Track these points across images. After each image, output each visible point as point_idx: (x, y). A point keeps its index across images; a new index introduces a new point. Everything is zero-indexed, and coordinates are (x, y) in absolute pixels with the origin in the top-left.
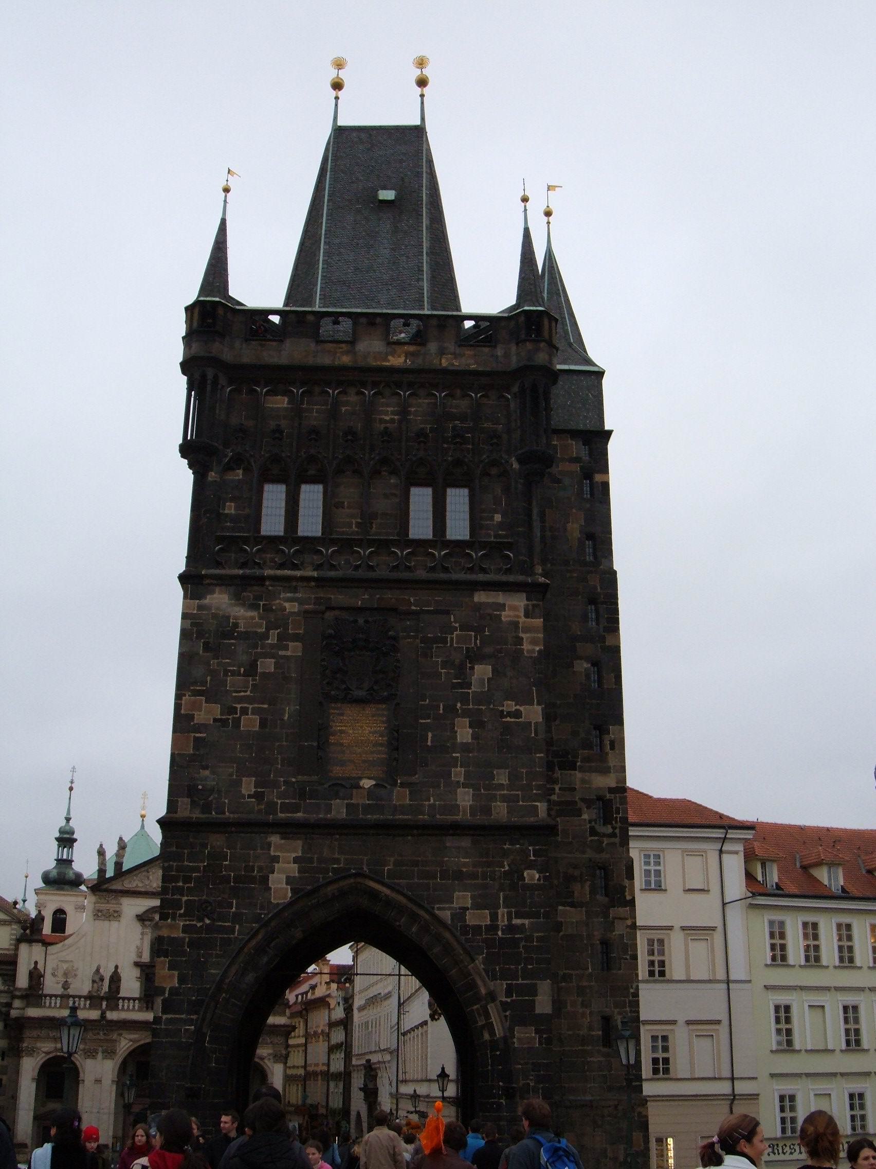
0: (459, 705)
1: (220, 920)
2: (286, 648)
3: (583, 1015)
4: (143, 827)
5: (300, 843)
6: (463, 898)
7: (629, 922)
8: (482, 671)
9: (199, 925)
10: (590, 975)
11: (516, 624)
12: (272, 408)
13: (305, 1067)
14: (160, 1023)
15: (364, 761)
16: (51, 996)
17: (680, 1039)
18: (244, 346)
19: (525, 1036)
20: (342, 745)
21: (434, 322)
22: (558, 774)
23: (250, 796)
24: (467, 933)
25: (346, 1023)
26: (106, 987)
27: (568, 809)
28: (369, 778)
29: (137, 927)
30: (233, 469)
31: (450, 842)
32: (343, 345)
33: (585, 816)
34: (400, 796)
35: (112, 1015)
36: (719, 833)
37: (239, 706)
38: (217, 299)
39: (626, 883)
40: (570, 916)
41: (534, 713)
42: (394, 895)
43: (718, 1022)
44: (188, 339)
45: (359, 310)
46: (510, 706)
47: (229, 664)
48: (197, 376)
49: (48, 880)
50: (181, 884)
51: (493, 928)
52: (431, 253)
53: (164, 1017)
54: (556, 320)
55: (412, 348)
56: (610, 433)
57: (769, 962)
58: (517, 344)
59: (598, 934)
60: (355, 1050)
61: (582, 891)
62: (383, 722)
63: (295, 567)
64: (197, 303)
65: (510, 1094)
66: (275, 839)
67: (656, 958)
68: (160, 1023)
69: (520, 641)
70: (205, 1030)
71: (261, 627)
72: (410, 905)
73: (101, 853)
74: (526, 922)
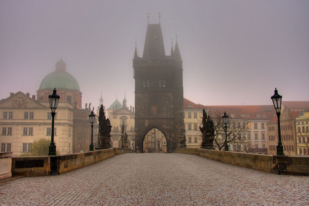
4: (117, 99)
6: (165, 126)
8: (167, 102)
13: (147, 141)
19: (171, 139)
25: (155, 133)
29: (120, 119)
31: (163, 120)
35: (117, 134)
41: (172, 106)
51: (168, 129)
56: (183, 69)
60: (156, 138)
65: (170, 145)
66: (146, 120)
74: (171, 128)
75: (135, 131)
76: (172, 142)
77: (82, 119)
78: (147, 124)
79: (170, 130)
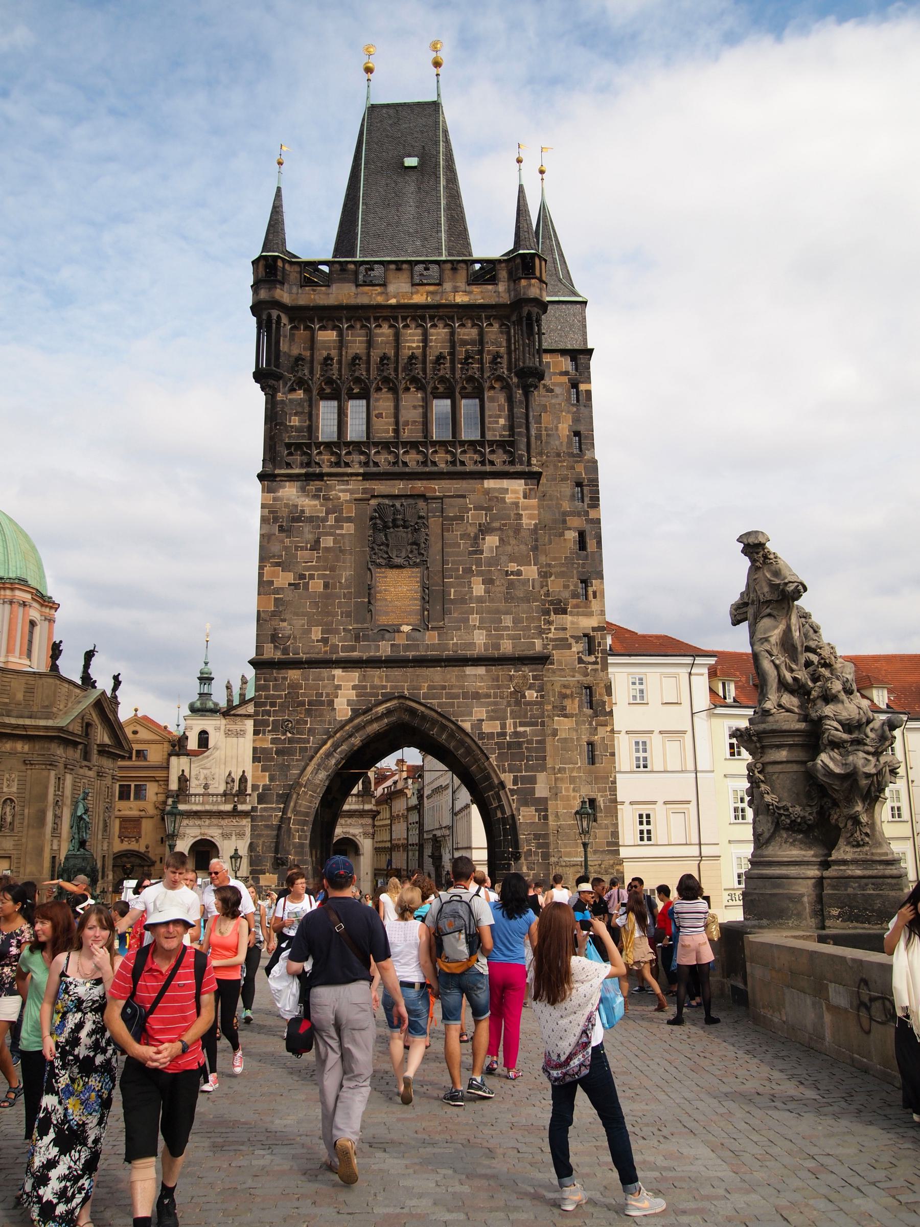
0: (474, 567)
1: (298, 733)
2: (342, 528)
3: (574, 798)
5: (357, 674)
7: (609, 729)
8: (491, 541)
9: (283, 738)
10: (580, 767)
11: (516, 504)
12: (325, 342)
13: (391, 841)
14: (256, 811)
15: (403, 612)
16: (195, 795)
17: (659, 814)
18: (300, 291)
20: (386, 600)
21: (449, 266)
22: (553, 617)
23: (318, 641)
24: (483, 738)
25: (419, 808)
26: (236, 788)
27: (563, 644)
28: (408, 625)
30: (295, 390)
31: (469, 670)
32: (377, 288)
33: (574, 649)
34: (431, 638)
35: (241, 807)
36: (689, 660)
37: (307, 573)
38: (276, 254)
39: (606, 698)
40: (563, 725)
41: (531, 572)
42: (427, 712)
43: (688, 802)
44: (256, 287)
45: (389, 259)
46: (513, 567)
47: (298, 542)
48: (264, 317)
49: (193, 710)
50: (268, 708)
51: (503, 734)
52: (448, 208)
53: (259, 806)
54: (546, 261)
55: (431, 288)
56: (592, 350)
57: (728, 756)
58: (514, 281)
59: (585, 738)
60: (426, 828)
61: (572, 706)
62: (417, 582)
63: (347, 465)
64: (261, 257)
66: (338, 672)
67: (641, 755)
68: (256, 811)
69: (519, 516)
70: (289, 815)
71: (322, 512)
72: (440, 719)
73: (228, 687)
74: (528, 729)
75: (255, 759)
76: (537, 837)
77: (28, 722)
78: (349, 703)
79: (519, 744)
